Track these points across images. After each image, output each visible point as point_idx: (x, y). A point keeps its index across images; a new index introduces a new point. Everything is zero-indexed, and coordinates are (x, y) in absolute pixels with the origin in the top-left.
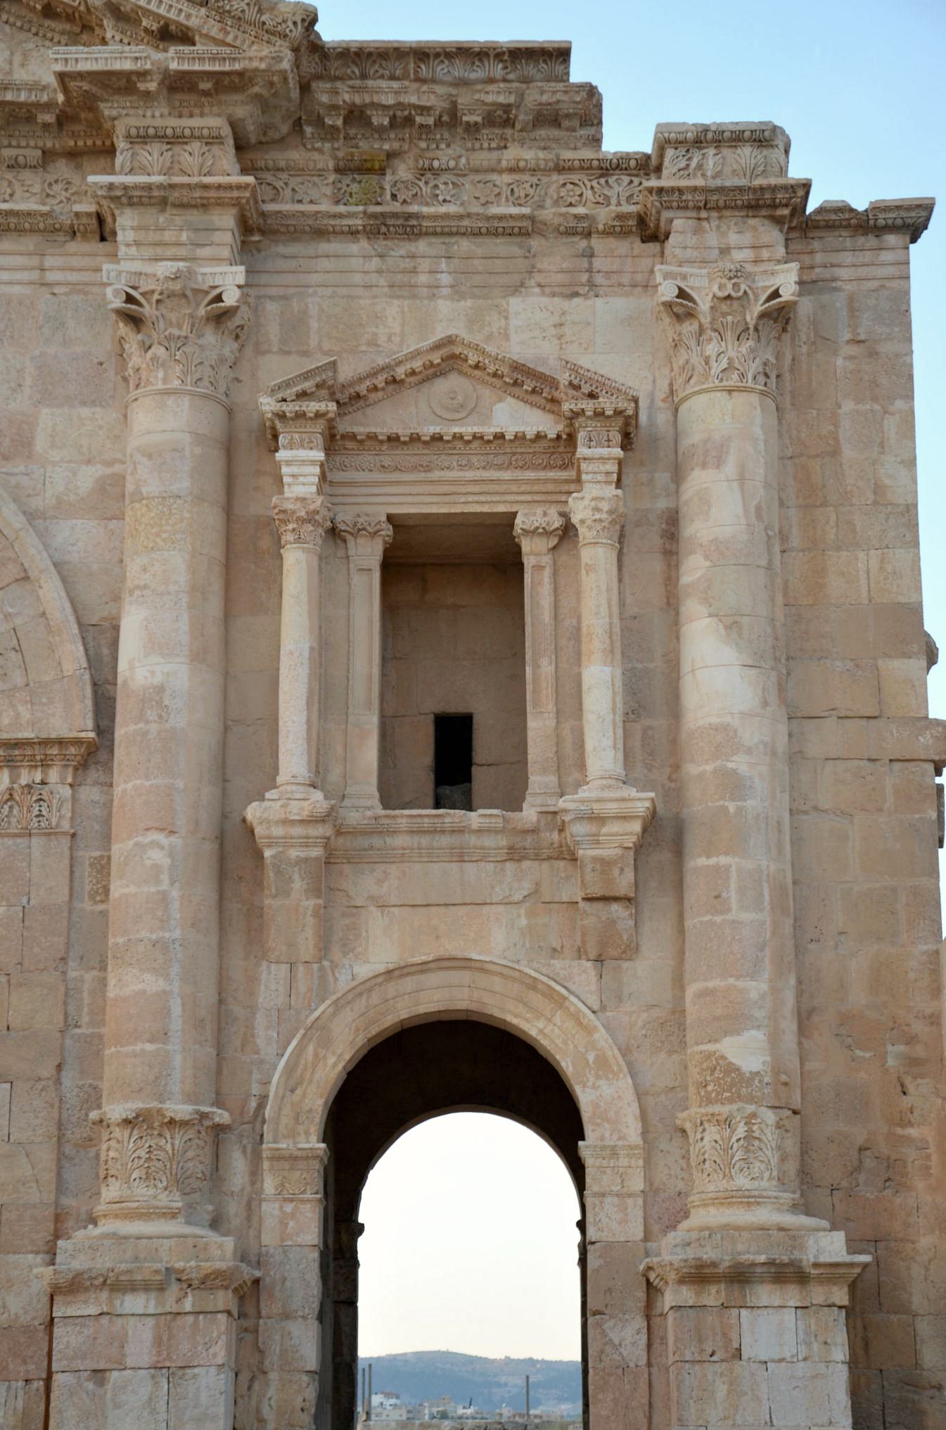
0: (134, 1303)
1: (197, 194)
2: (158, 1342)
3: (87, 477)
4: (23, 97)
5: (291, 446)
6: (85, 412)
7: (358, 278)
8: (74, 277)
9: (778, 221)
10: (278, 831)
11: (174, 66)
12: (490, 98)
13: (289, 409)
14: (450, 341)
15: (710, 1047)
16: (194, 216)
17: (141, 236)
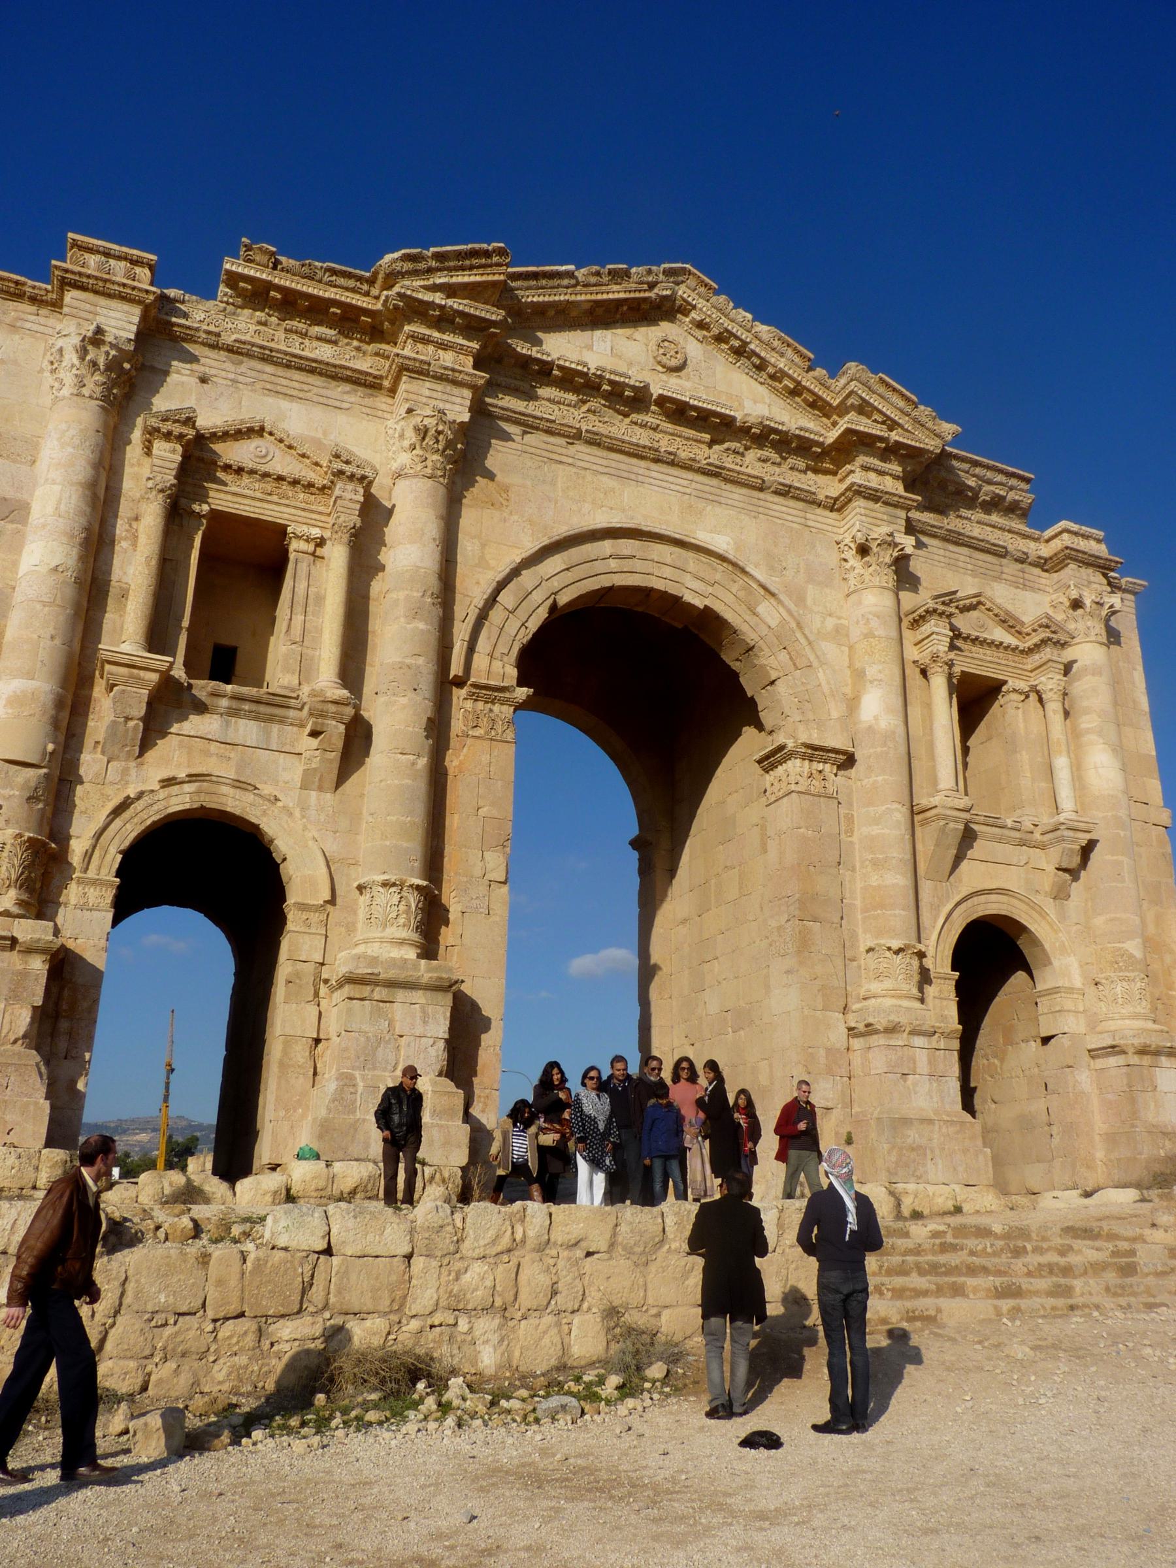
0: (919, 1041)
1: (896, 499)
2: (930, 1062)
3: (830, 623)
4: (812, 436)
5: (936, 625)
6: (827, 591)
7: (936, 557)
8: (819, 525)
9: (1105, 575)
10: (949, 812)
11: (897, 438)
12: (997, 491)
13: (941, 608)
14: (978, 595)
15: (1118, 945)
16: (890, 509)
17: (867, 512)
